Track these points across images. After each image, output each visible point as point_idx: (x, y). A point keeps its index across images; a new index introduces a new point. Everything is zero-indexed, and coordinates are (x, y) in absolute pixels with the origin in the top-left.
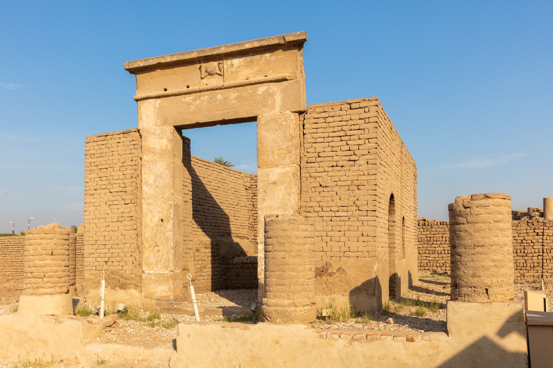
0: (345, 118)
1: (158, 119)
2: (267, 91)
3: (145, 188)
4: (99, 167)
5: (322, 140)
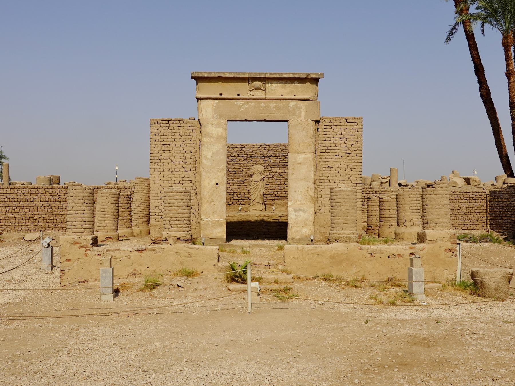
0: (343, 127)
2: (296, 105)
3: (204, 161)
4: (162, 143)
5: (329, 139)
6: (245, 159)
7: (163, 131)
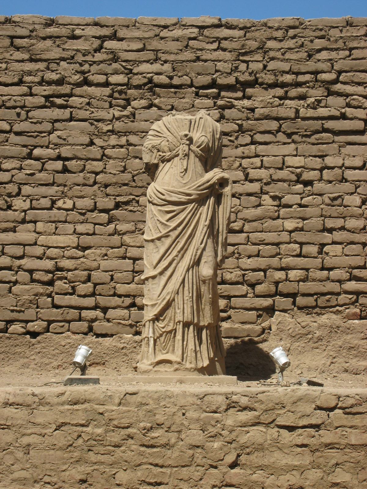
6: (120, 95)
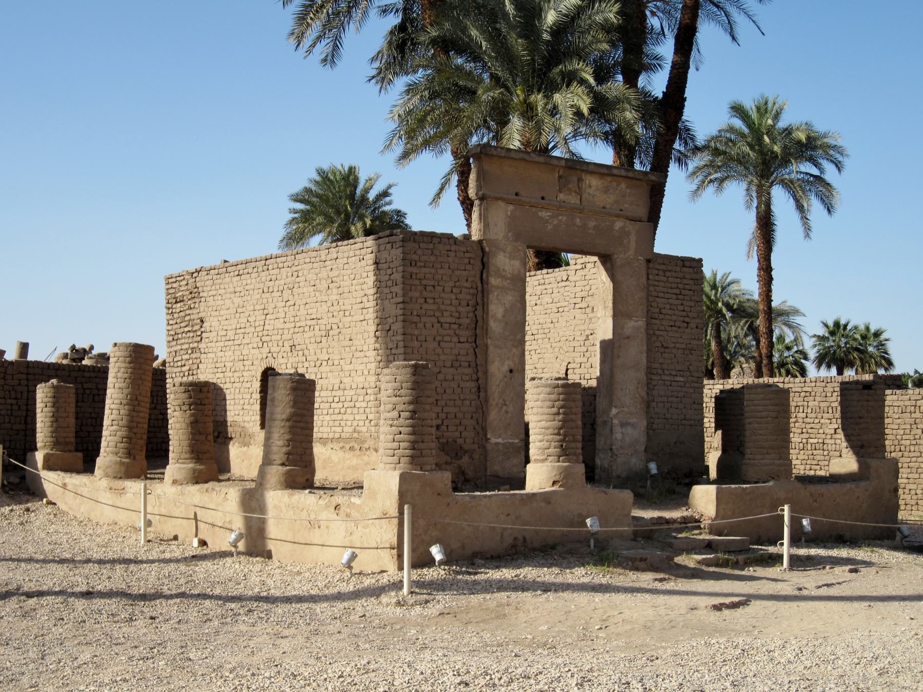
1: (509, 231)
4: (424, 282)
7: (424, 258)
